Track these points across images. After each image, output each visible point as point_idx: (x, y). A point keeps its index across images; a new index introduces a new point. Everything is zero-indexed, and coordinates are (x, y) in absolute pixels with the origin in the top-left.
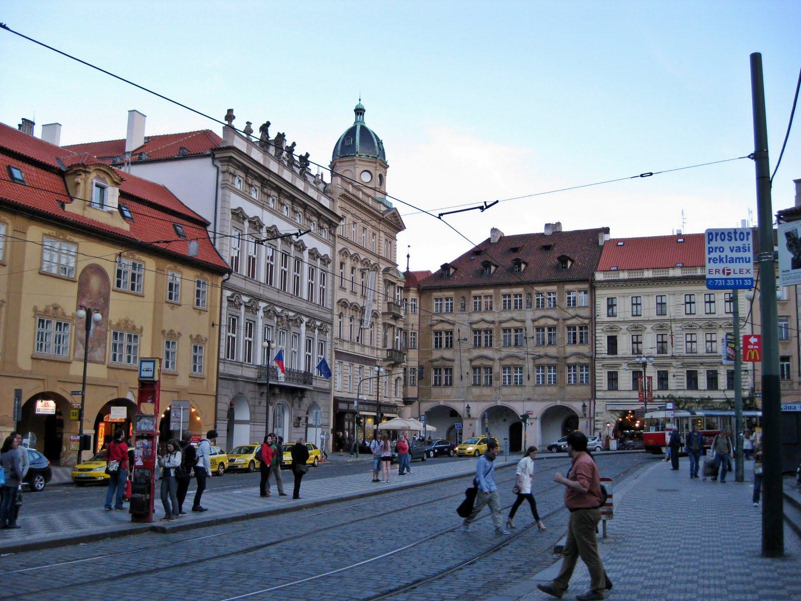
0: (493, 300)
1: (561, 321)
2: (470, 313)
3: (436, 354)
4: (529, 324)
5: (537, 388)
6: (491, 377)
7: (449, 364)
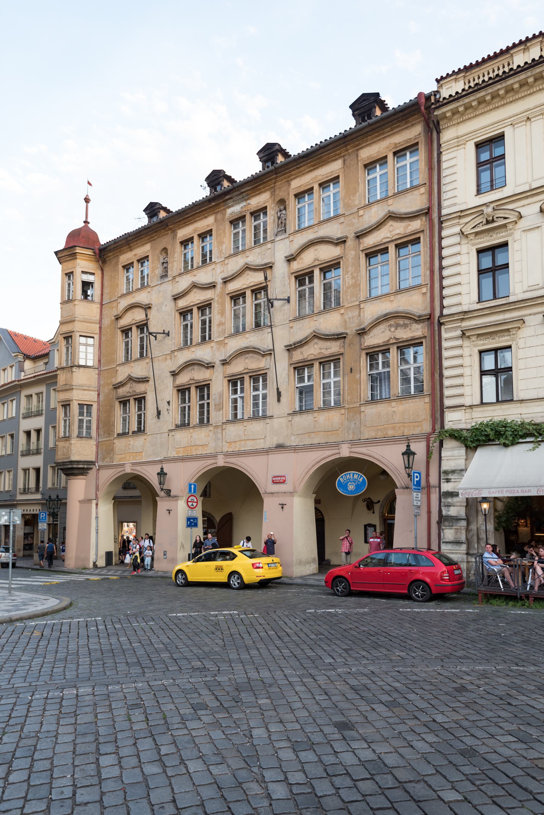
1: (350, 243)
2: (174, 278)
3: (122, 374)
4: (281, 270)
5: (297, 419)
7: (140, 388)
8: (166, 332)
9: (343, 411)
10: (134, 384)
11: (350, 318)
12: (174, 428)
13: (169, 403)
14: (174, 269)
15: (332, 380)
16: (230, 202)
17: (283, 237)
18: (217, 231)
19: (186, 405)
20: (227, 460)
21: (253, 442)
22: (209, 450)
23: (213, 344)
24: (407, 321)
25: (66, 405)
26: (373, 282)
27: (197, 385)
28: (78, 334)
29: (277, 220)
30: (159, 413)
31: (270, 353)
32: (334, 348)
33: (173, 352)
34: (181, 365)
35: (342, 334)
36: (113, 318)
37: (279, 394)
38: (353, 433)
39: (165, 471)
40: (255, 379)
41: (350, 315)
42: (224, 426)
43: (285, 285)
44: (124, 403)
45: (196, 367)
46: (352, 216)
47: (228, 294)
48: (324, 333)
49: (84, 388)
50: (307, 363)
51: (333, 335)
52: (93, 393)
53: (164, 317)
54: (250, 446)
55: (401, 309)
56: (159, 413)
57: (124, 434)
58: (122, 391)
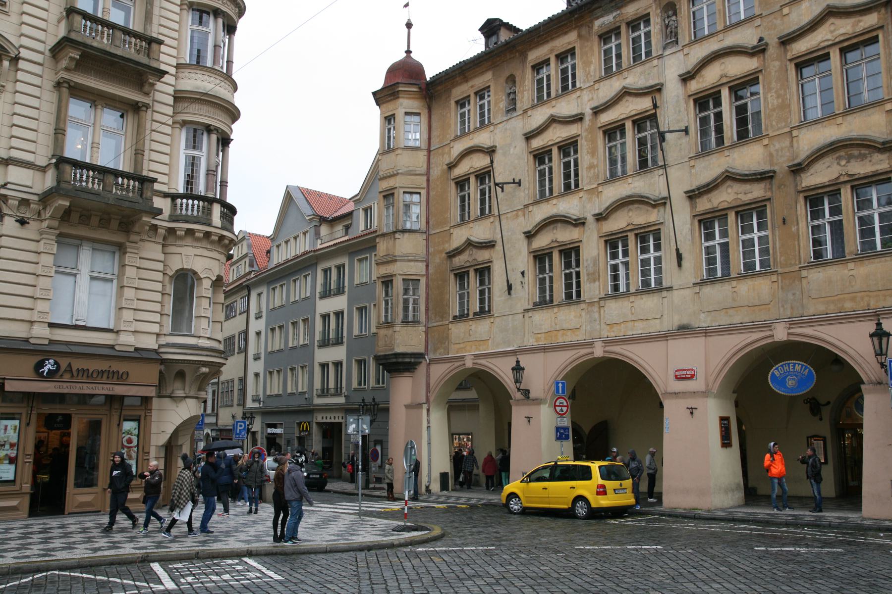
0: (577, 61)
1: (773, 50)
2: (525, 111)
3: (459, 237)
5: (707, 290)
6: (578, 274)
7: (482, 256)
8: (517, 180)
9: (774, 278)
10: (475, 250)
11: (777, 151)
13: (523, 273)
14: (525, 100)
15: (756, 235)
16: (598, 12)
17: (674, 49)
18: (581, 49)
19: (573, 271)
20: (607, 349)
21: (645, 323)
22: (580, 337)
23: (581, 194)
24: (864, 151)
25: (387, 282)
26: (807, 99)
27: (561, 248)
28: (402, 191)
29: (664, 29)
30: (510, 287)
31: (663, 202)
32: (757, 191)
33: (526, 206)
34: (539, 224)
35: (768, 172)
36: (445, 167)
37: (679, 257)
38: (792, 308)
39: (522, 365)
40: (642, 238)
41: (777, 146)
42: (602, 303)
43: (680, 111)
44: (461, 276)
45: (559, 225)
46: (772, 16)
47: (600, 128)
48: (740, 172)
49: (410, 258)
50: (717, 214)
51: (755, 174)
52: (420, 264)
53: (513, 162)
54: (639, 329)
55: (854, 134)
56: (510, 287)
57: (462, 317)
58: (459, 261)
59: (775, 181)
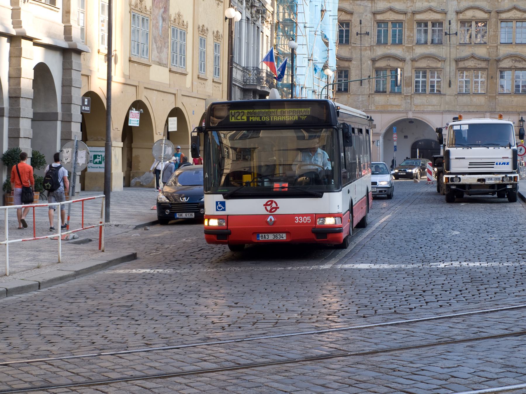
4: (451, 16)
9: (486, 97)
12: (373, 92)
20: (414, 115)
23: (404, 48)
32: (483, 65)
42: (413, 96)
45: (391, 59)
59: (490, 62)
